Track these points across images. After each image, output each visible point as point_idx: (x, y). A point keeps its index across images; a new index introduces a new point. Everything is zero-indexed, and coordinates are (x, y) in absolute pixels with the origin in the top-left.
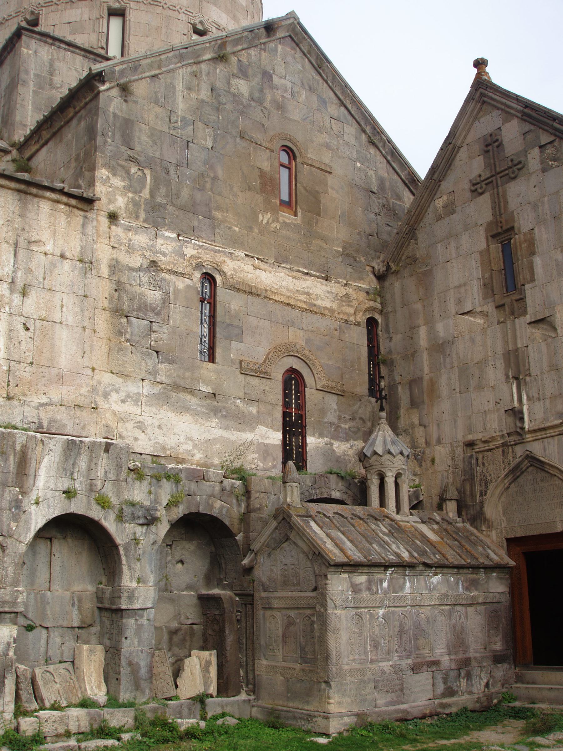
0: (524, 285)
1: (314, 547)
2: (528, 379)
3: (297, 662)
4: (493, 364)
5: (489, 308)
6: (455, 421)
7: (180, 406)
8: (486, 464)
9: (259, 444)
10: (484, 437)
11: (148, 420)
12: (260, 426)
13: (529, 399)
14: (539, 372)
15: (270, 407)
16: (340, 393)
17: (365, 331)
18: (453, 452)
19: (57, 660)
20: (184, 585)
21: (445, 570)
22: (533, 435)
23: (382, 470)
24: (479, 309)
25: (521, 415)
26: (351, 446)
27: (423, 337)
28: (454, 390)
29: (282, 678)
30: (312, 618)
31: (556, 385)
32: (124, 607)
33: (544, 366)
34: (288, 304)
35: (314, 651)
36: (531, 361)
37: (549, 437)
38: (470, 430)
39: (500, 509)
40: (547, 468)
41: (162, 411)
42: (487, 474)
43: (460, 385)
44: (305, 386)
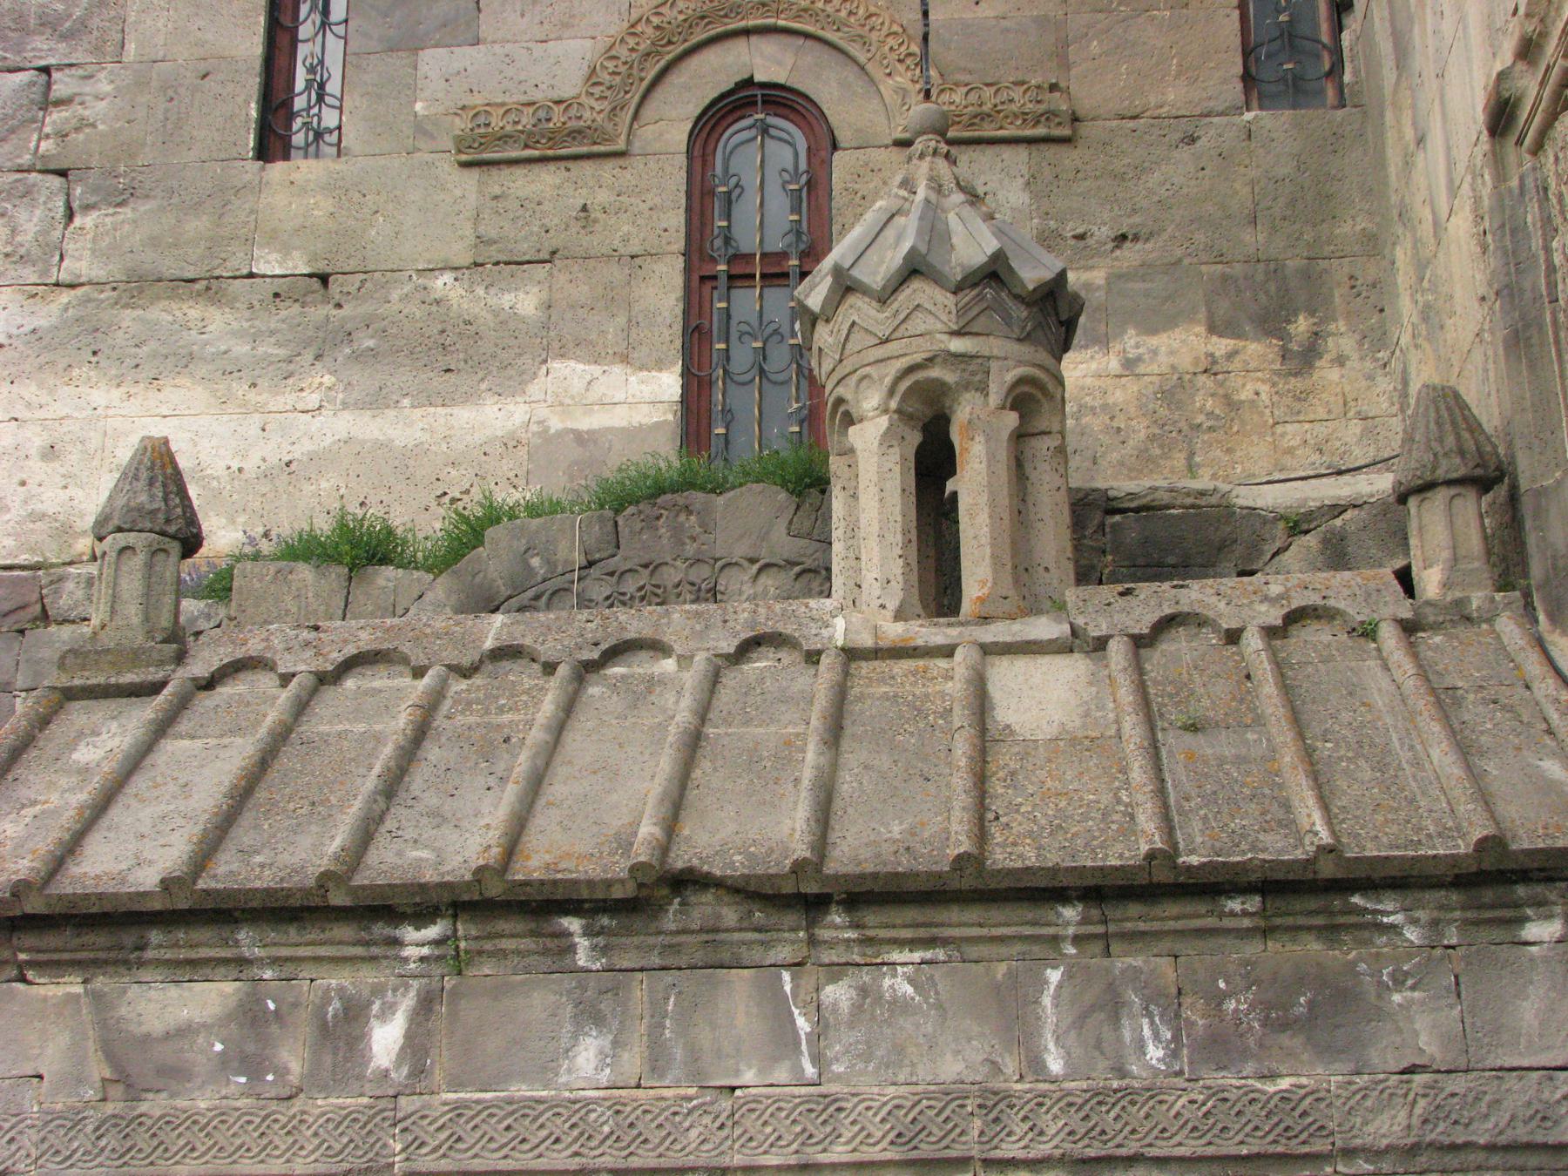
7: (154, 355)
12: (555, 365)
15: (616, 273)
16: (1041, 131)
21: (961, 921)
26: (1130, 364)
38: (1493, 33)
41: (65, 391)
44: (835, 147)
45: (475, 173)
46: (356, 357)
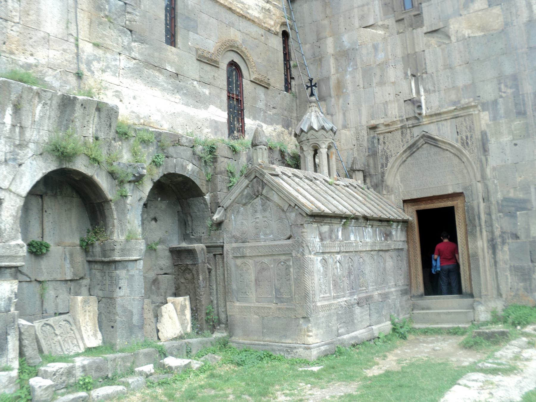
0: (421, 4)
1: (290, 200)
2: (424, 76)
3: (272, 302)
4: (393, 65)
5: (390, 21)
6: (360, 110)
8: (387, 143)
9: (212, 121)
10: (385, 121)
11: (124, 92)
12: (211, 105)
13: (425, 91)
14: (434, 71)
15: (218, 90)
16: (266, 86)
17: (281, 40)
18: (357, 134)
19: (52, 312)
20: (157, 240)
22: (429, 119)
23: (317, 142)
24: (380, 23)
25: (419, 104)
26: (275, 129)
27: (330, 46)
28: (358, 86)
29: (256, 316)
30: (288, 263)
31: (450, 80)
32: (118, 258)
34: (230, 9)
35: (290, 292)
36: (428, 61)
37: (444, 120)
38: (372, 117)
39: (398, 178)
40: (440, 145)
42: (388, 151)
43: (363, 82)
45: (198, 62)
46: (185, 94)
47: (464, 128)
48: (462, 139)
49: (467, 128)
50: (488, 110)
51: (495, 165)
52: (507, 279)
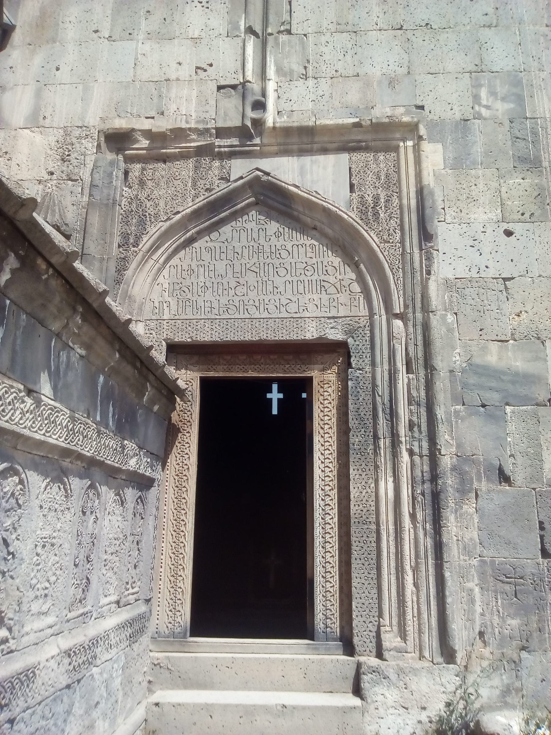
2: (284, 38)
6: (86, 89)
8: (150, 184)
13: (279, 71)
33: (325, 24)
47: (370, 178)
48: (362, 200)
49: (379, 178)
50: (442, 140)
51: (451, 276)
52: (472, 601)
